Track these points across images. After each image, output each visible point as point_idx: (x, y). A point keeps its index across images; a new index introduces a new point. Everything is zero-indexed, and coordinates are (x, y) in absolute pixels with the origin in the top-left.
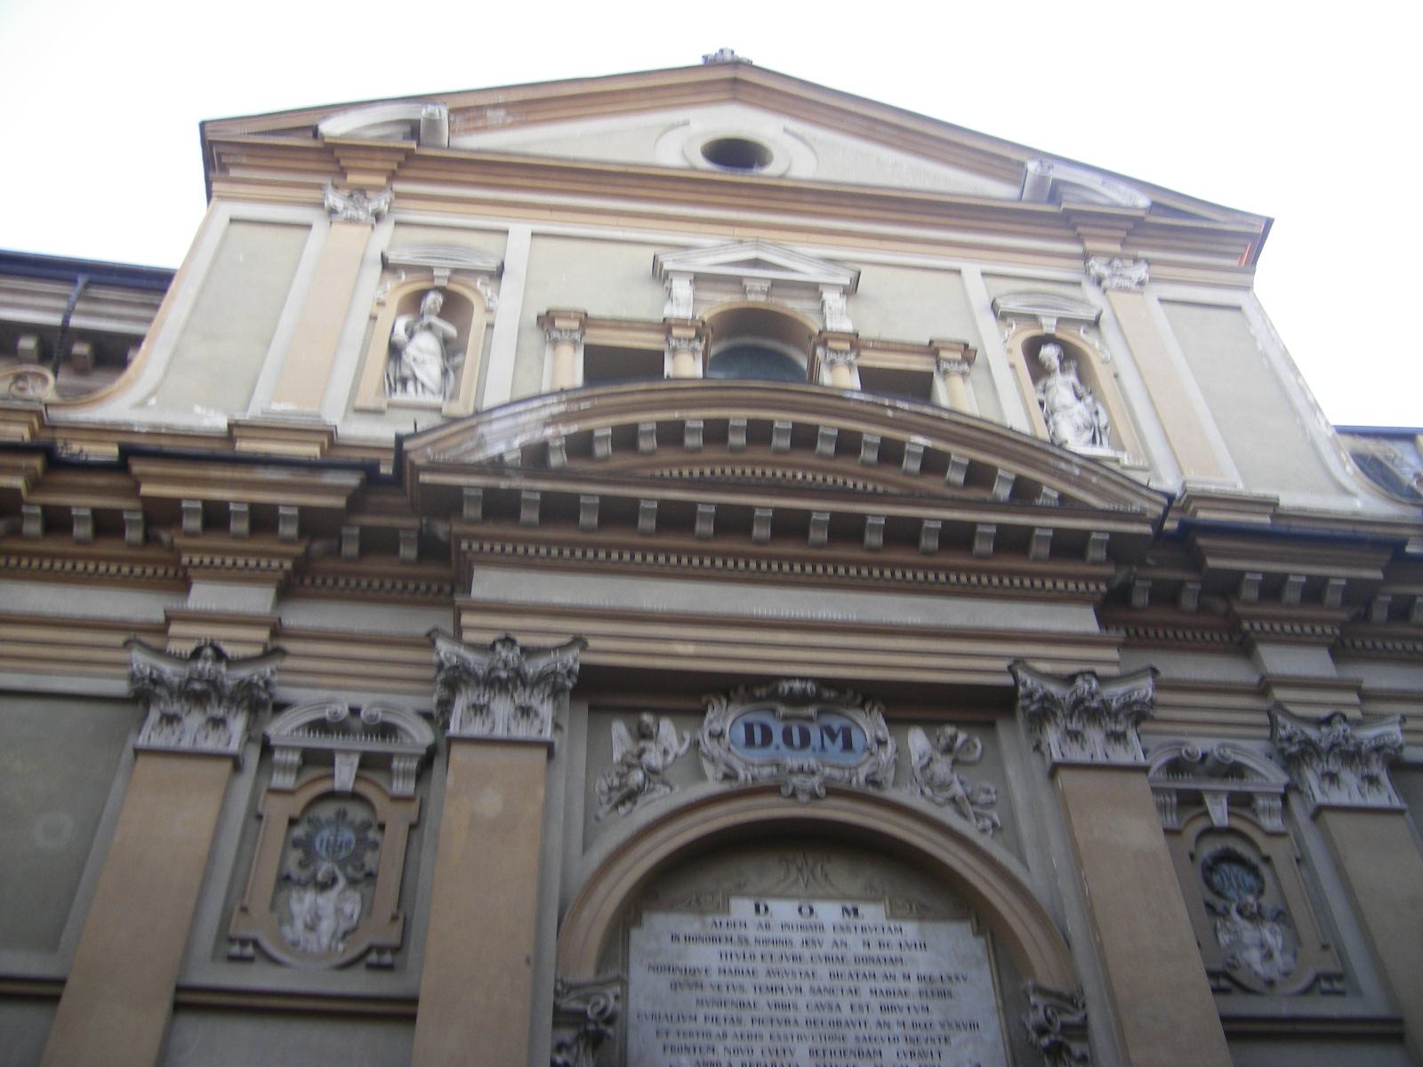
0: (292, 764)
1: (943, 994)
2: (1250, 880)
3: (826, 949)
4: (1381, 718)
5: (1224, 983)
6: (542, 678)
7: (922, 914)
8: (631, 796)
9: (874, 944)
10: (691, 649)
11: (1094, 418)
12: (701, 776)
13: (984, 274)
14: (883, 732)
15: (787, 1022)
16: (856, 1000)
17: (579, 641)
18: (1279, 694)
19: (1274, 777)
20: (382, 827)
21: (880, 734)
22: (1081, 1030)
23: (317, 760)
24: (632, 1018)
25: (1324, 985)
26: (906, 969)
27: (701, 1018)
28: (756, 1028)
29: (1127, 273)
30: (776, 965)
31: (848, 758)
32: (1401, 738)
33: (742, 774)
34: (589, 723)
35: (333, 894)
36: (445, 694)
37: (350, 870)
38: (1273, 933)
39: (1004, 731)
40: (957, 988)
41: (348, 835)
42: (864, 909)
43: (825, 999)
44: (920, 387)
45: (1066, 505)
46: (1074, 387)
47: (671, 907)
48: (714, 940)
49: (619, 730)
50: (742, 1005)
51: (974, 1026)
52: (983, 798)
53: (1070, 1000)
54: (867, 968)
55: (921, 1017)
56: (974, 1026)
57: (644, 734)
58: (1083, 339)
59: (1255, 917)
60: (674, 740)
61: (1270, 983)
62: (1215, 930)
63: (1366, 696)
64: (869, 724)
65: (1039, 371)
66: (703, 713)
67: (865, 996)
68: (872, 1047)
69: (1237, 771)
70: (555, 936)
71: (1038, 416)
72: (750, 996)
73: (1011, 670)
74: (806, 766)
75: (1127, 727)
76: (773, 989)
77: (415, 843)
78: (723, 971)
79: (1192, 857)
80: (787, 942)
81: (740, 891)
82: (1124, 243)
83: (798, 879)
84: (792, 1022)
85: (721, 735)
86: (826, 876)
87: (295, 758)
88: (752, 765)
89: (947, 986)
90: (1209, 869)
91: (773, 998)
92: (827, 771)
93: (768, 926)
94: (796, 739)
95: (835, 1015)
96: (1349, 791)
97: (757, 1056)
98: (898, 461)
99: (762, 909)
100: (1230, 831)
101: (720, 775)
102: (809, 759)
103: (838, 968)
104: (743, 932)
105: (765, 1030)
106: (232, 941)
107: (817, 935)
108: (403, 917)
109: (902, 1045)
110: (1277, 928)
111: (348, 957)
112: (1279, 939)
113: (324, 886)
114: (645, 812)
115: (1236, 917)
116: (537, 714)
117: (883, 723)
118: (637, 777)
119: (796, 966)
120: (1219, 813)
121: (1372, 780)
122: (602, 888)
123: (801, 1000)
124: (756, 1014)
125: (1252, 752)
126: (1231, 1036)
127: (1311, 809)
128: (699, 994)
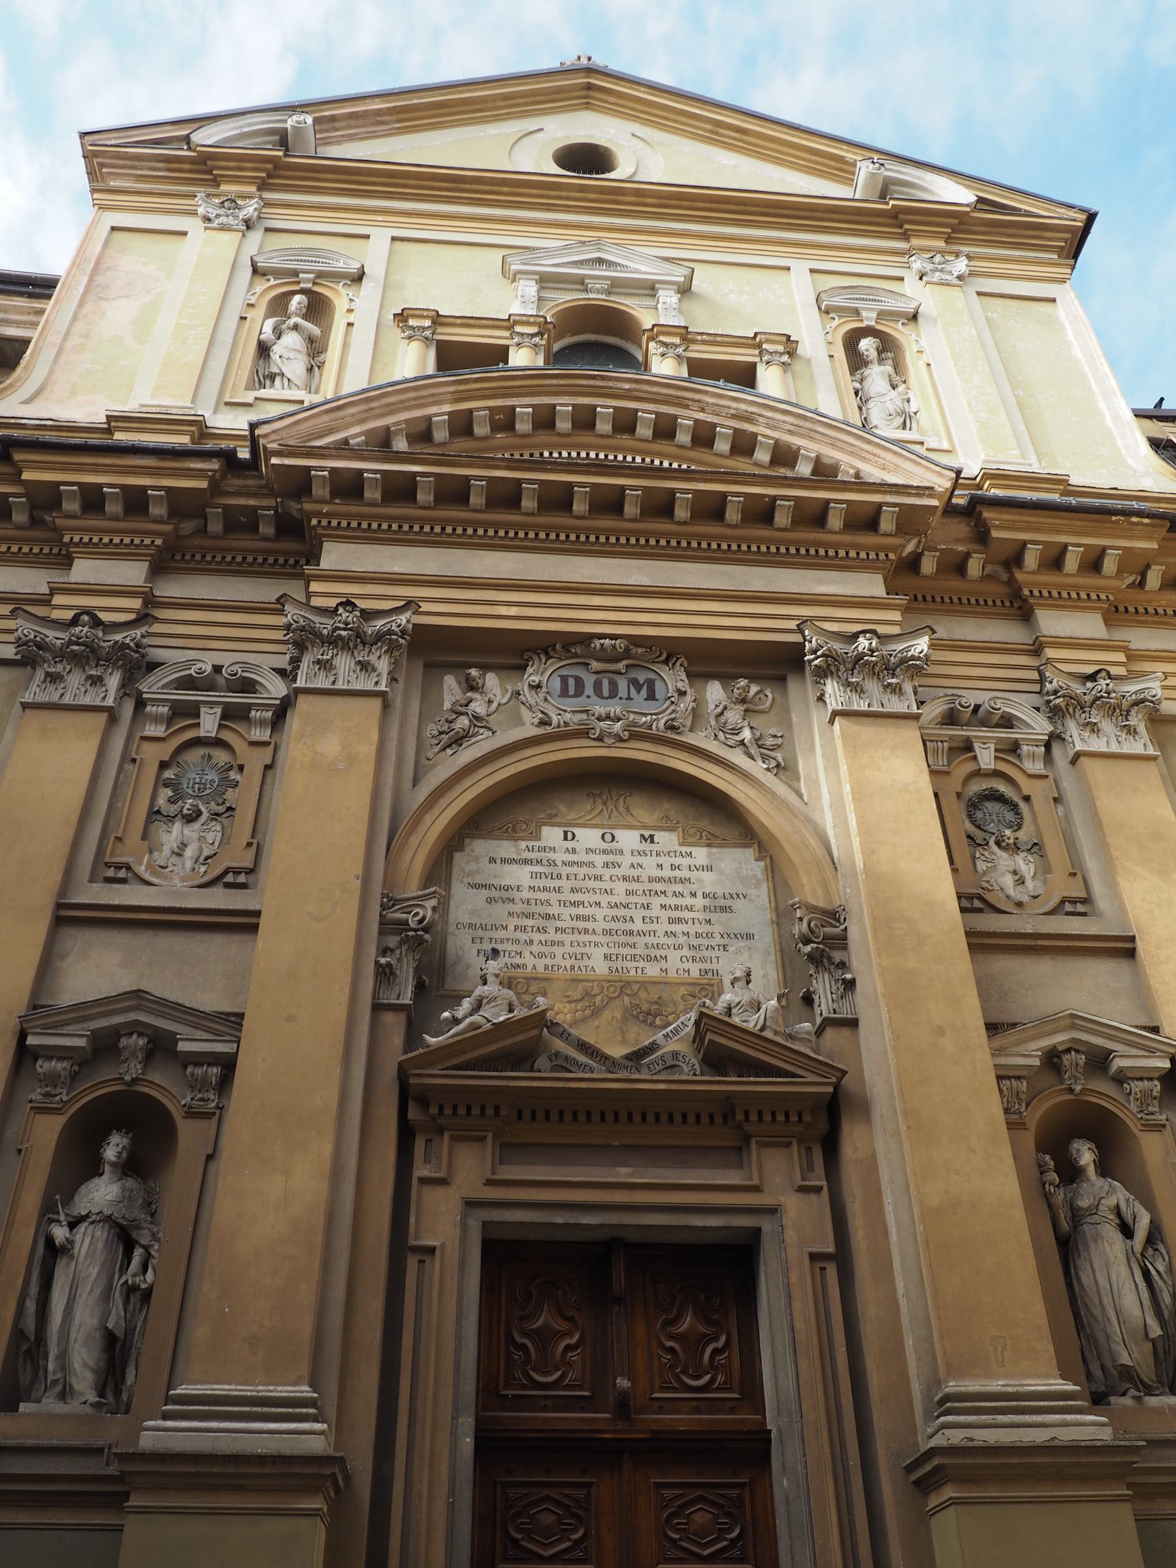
0: (162, 715)
1: (724, 909)
2: (1010, 816)
3: (624, 870)
4: (1143, 674)
5: (977, 904)
6: (380, 637)
7: (711, 842)
8: (458, 740)
9: (666, 866)
10: (513, 611)
11: (906, 404)
12: (521, 723)
13: (812, 271)
14: (683, 685)
15: (586, 931)
16: (647, 913)
17: (410, 604)
18: (1050, 653)
19: (1041, 726)
20: (241, 768)
21: (680, 685)
22: (841, 941)
23: (187, 712)
24: (452, 928)
25: (1068, 907)
26: (693, 888)
27: (511, 928)
28: (559, 937)
29: (948, 267)
30: (578, 885)
31: (651, 707)
32: (1159, 692)
33: (555, 720)
34: (424, 675)
35: (196, 825)
36: (296, 653)
37: (213, 805)
38: (1027, 863)
39: (793, 685)
40: (738, 904)
41: (212, 776)
42: (660, 836)
43: (621, 912)
44: (746, 376)
45: (860, 484)
46: (890, 376)
47: (489, 835)
48: (526, 862)
49: (450, 683)
50: (547, 917)
51: (750, 936)
52: (770, 742)
53: (834, 916)
54: (659, 887)
55: (703, 929)
56: (750, 936)
57: (472, 686)
58: (898, 331)
59: (1015, 848)
60: (498, 692)
61: (1019, 904)
62: (974, 858)
63: (1133, 656)
64: (673, 679)
65: (857, 362)
66: (523, 668)
67: (655, 911)
68: (659, 953)
69: (1007, 722)
70: (384, 855)
71: (853, 402)
72: (554, 910)
73: (800, 630)
74: (612, 714)
75: (903, 680)
76: (575, 904)
77: (269, 781)
78: (532, 888)
79: (959, 795)
80: (591, 864)
81: (551, 821)
82: (949, 240)
83: (602, 810)
84: (591, 931)
85: (539, 686)
86: (627, 809)
87: (164, 710)
88: (564, 712)
89: (728, 903)
90: (973, 805)
91: (574, 911)
92: (632, 717)
93: (574, 851)
94: (606, 692)
95: (628, 926)
96: (1108, 739)
97: (558, 961)
98: (750, 452)
99: (570, 836)
100: (997, 774)
101: (536, 721)
102: (615, 708)
103: (634, 886)
104: (552, 855)
105: (567, 938)
106: (108, 865)
107: (617, 858)
108: (256, 846)
109: (685, 952)
110: (1030, 858)
111: (206, 879)
112: (1032, 866)
113: (191, 818)
114: (467, 755)
115: (995, 848)
116: (374, 670)
117: (684, 676)
118: (463, 722)
119: (597, 885)
120: (986, 758)
121: (1131, 731)
122: (428, 819)
123: (600, 913)
124: (559, 924)
125: (1022, 707)
126: (972, 947)
127: (1071, 754)
128: (511, 907)
